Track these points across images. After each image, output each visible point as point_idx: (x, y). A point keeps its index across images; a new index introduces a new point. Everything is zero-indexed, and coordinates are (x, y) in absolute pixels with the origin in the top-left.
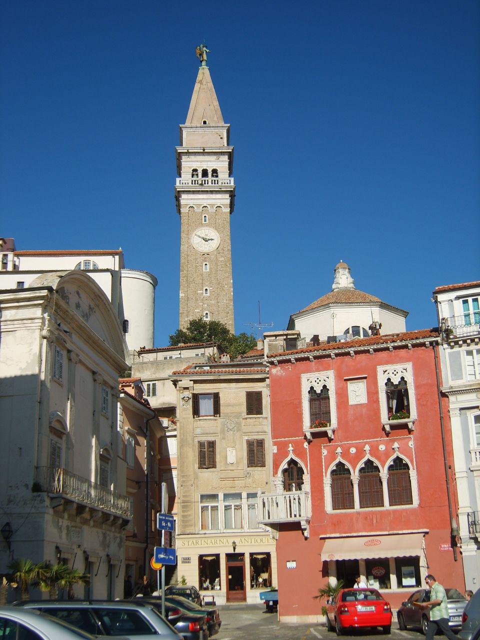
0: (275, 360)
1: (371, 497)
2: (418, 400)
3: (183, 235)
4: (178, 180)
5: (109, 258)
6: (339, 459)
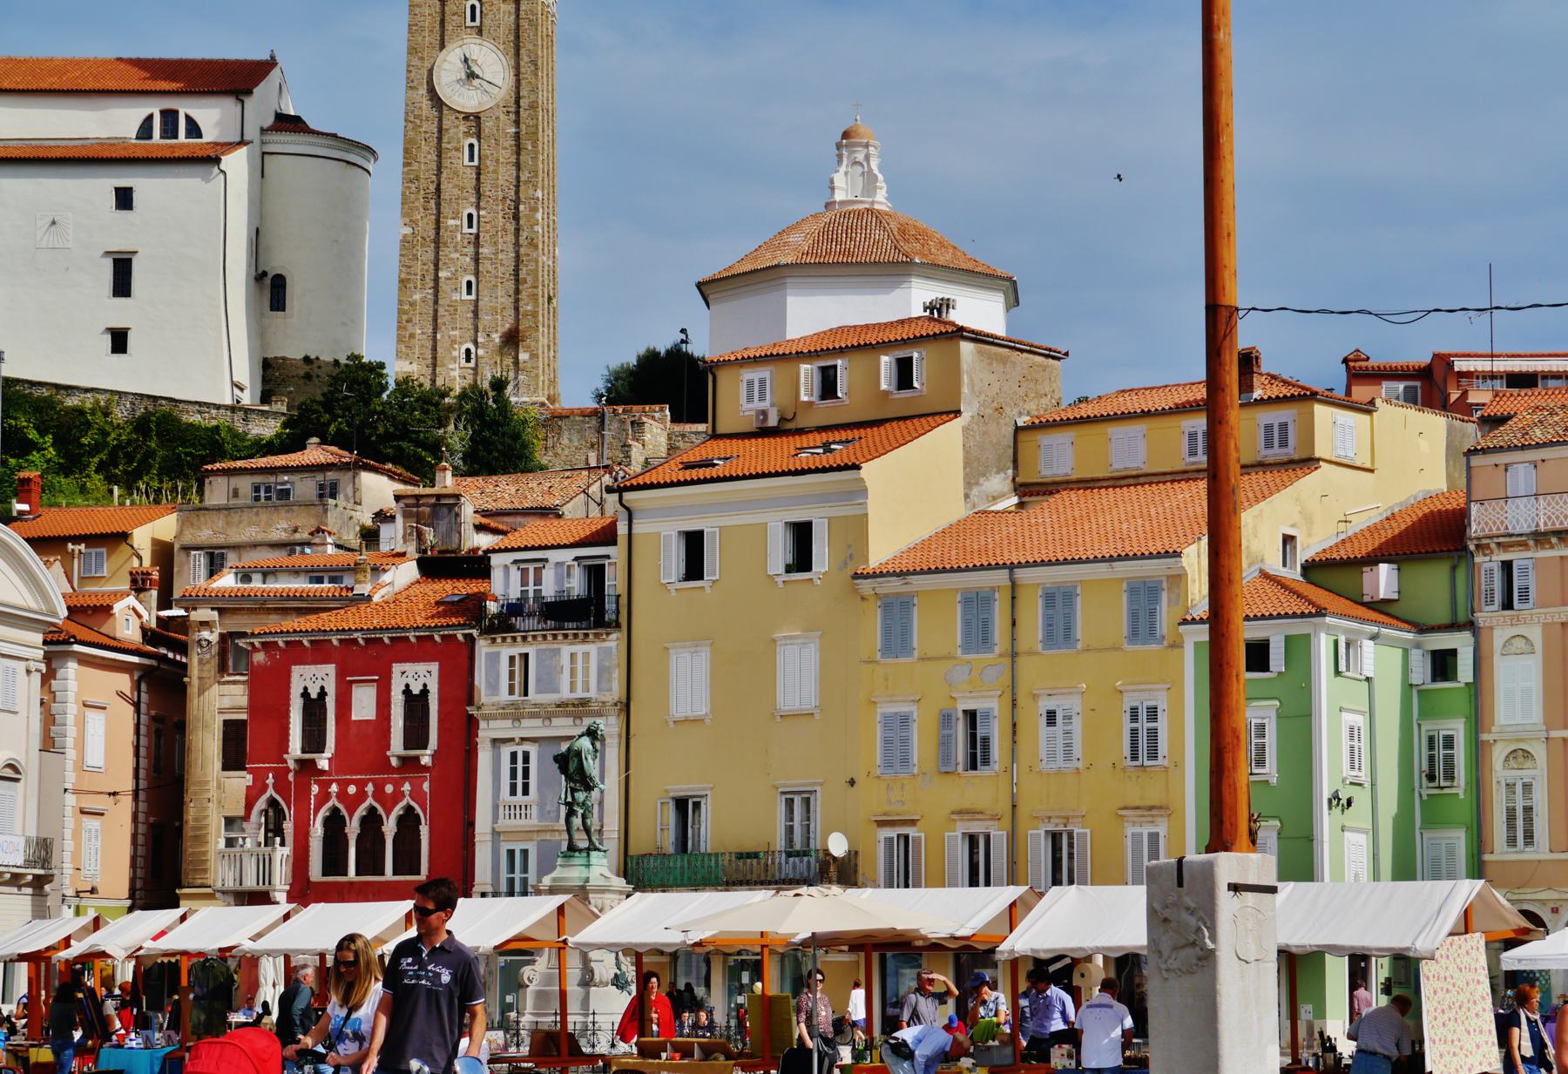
0: (256, 642)
1: (370, 860)
2: (441, 721)
6: (334, 801)
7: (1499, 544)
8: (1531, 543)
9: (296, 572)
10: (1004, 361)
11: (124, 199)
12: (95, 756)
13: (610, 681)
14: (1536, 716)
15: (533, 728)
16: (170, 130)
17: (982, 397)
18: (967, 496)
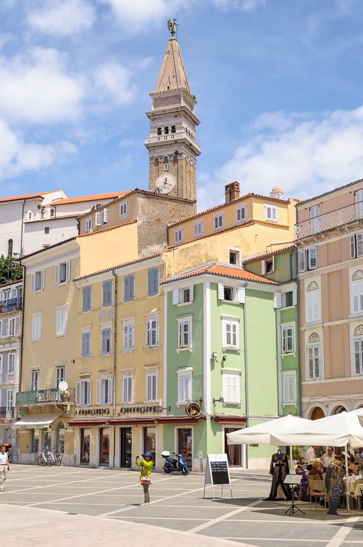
7: (305, 242)
8: (315, 239)
13: (18, 329)
14: (320, 318)
17: (149, 216)
18: (139, 252)
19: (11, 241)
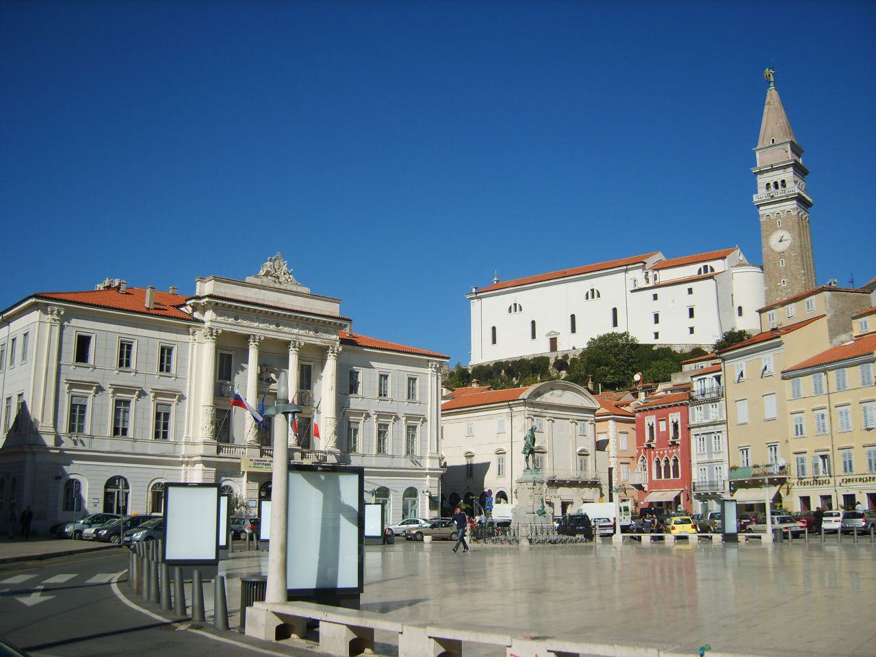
1: (667, 475)
3: (763, 240)
4: (754, 196)
5: (720, 261)
9: (680, 390)
10: (843, 296)
11: (690, 291)
12: (623, 446)
15: (704, 430)
16: (706, 270)
18: (831, 342)
19: (615, 310)
